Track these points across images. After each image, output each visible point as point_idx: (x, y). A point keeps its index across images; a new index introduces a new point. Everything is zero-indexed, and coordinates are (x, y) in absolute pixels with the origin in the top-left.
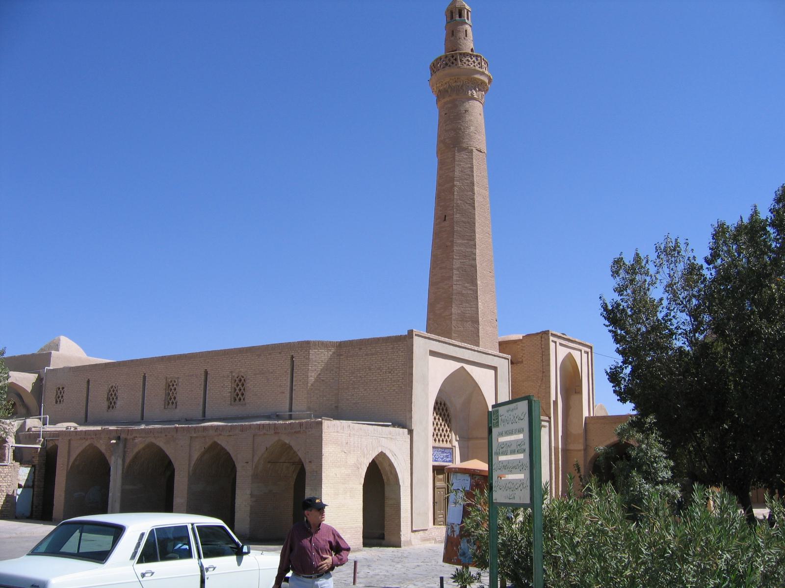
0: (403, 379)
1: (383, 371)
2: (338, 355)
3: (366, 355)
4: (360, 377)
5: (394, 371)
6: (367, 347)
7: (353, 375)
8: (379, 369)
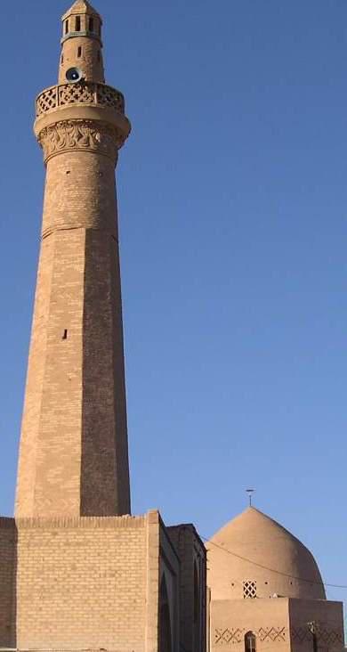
0: (137, 587)
1: (99, 572)
3: (67, 544)
4: (56, 580)
5: (120, 575)
6: (67, 532)
7: (42, 576)
8: (91, 569)
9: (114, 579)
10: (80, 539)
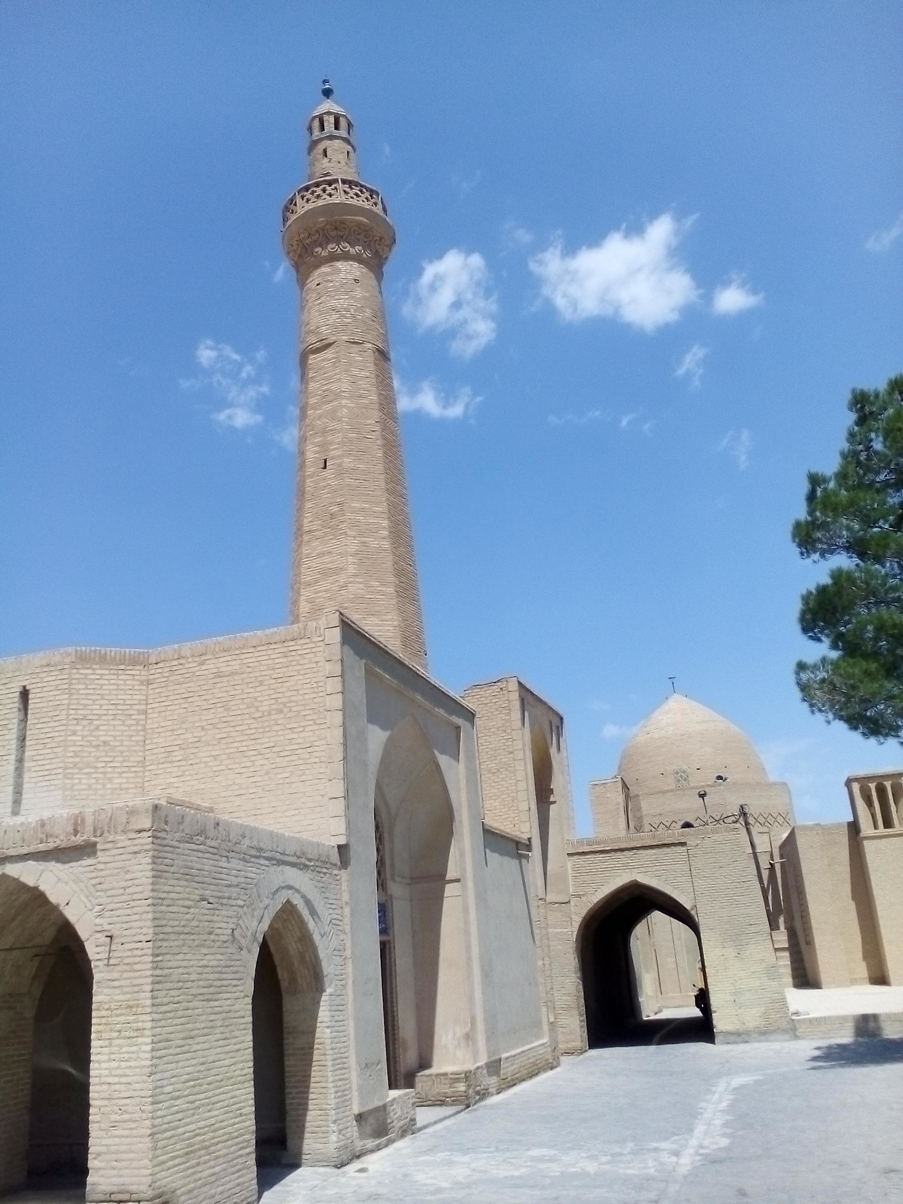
2: (142, 683)
9: (282, 716)
10: (235, 665)
